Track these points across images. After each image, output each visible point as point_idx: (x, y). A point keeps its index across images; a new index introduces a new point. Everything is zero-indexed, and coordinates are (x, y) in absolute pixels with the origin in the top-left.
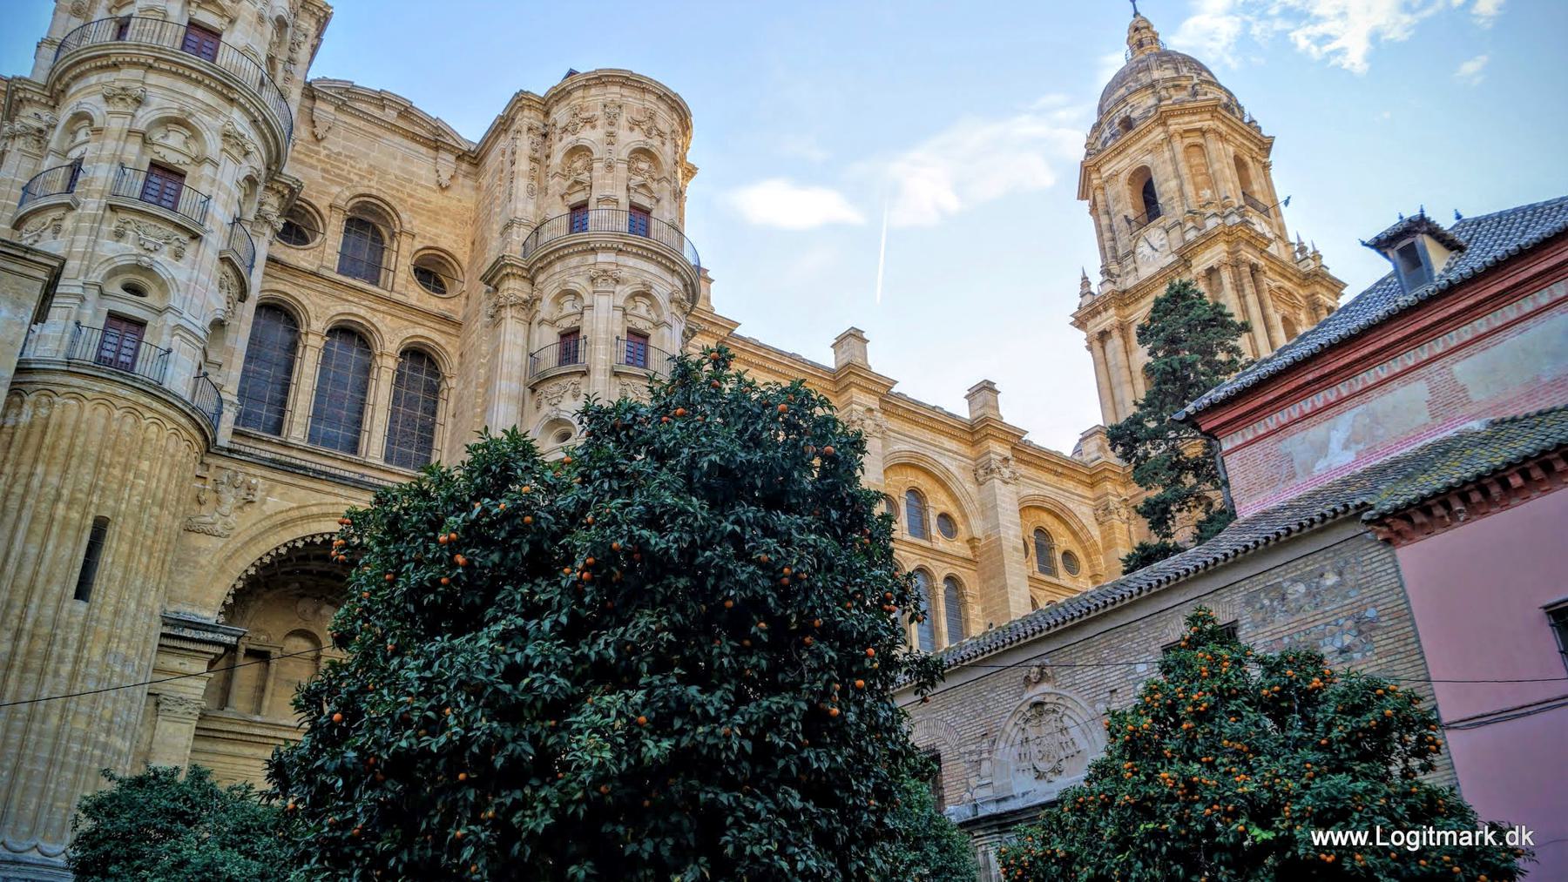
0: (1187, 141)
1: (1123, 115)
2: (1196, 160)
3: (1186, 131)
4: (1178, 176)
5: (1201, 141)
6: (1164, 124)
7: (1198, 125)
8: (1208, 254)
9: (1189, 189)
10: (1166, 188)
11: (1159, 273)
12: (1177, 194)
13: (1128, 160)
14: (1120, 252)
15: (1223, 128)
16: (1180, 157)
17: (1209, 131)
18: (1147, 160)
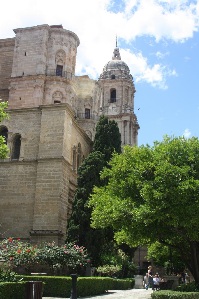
0: (126, 88)
1: (113, 74)
2: (126, 93)
3: (126, 86)
4: (122, 95)
5: (128, 89)
6: (122, 82)
7: (128, 85)
8: (126, 117)
9: (124, 99)
10: (119, 96)
11: (114, 115)
12: (121, 99)
13: (112, 85)
14: (105, 105)
15: (131, 87)
16: (124, 91)
17: (130, 88)
18: (116, 88)
